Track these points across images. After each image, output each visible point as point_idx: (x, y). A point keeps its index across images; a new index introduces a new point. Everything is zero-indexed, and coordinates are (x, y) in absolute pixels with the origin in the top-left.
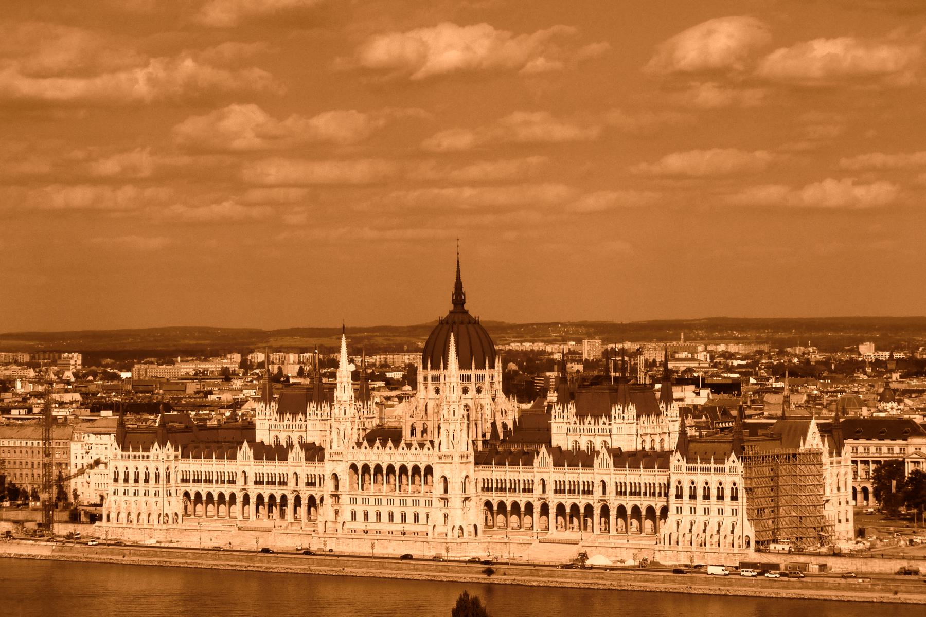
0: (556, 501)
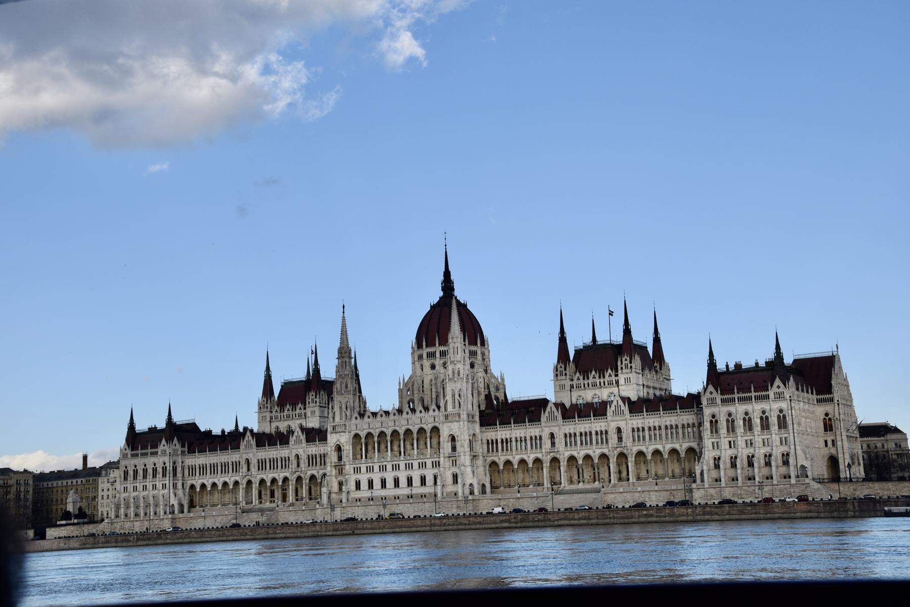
0: (567, 454)
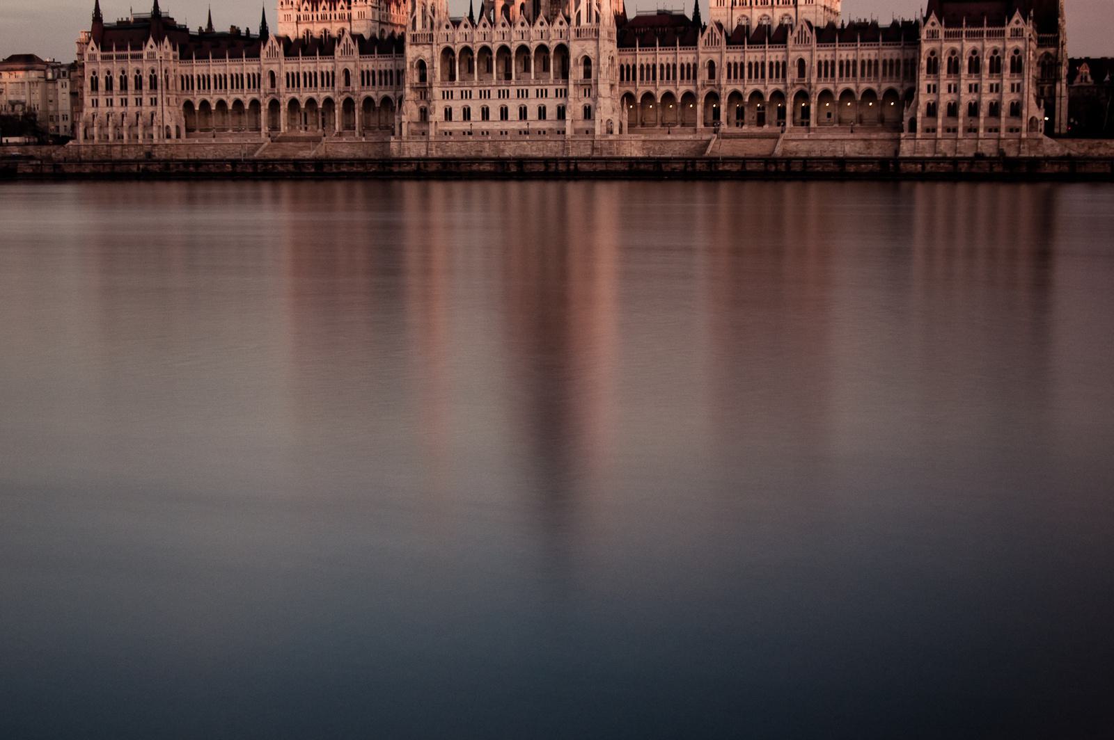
0: (730, 89)
